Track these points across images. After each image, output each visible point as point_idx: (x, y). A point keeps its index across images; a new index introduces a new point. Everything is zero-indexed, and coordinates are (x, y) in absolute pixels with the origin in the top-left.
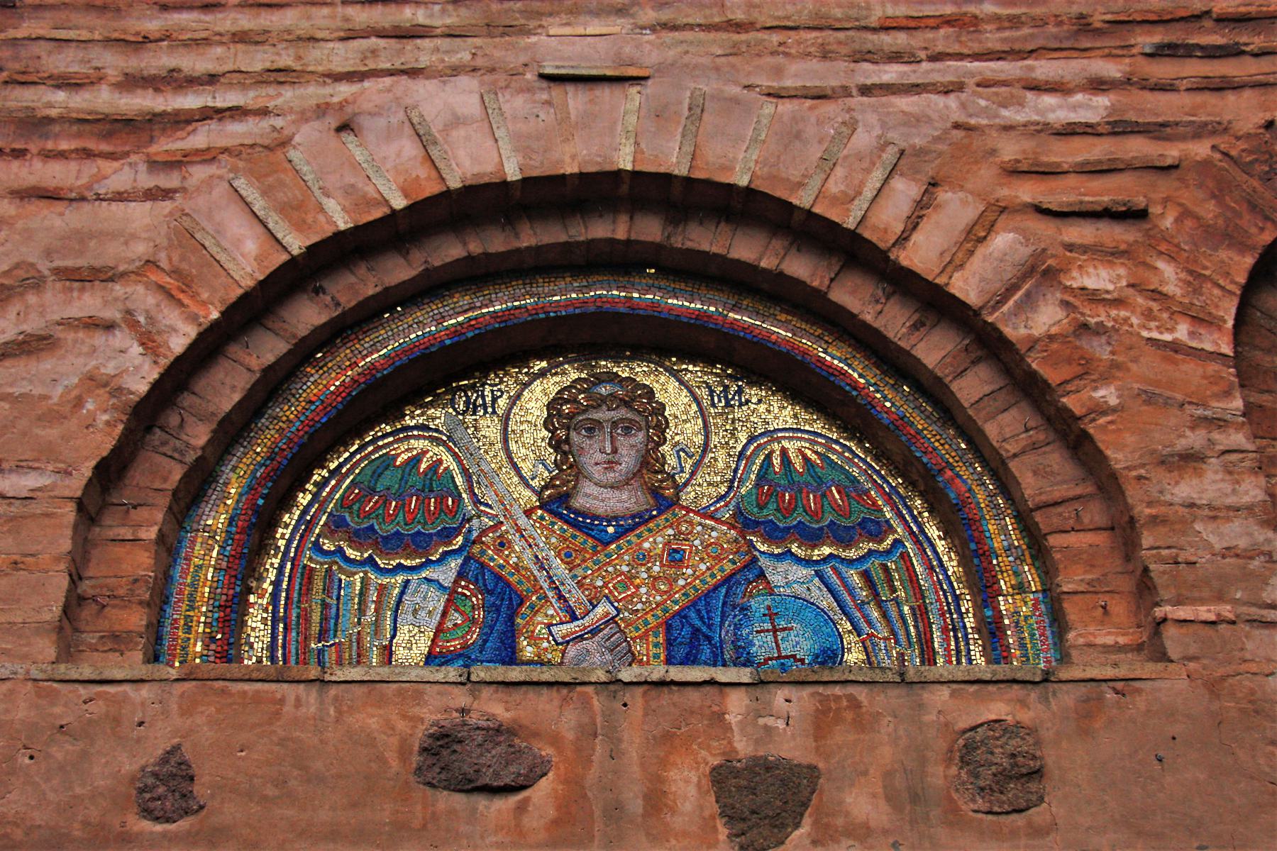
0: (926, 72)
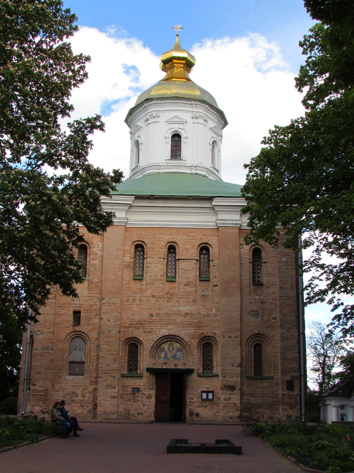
0: (187, 329)
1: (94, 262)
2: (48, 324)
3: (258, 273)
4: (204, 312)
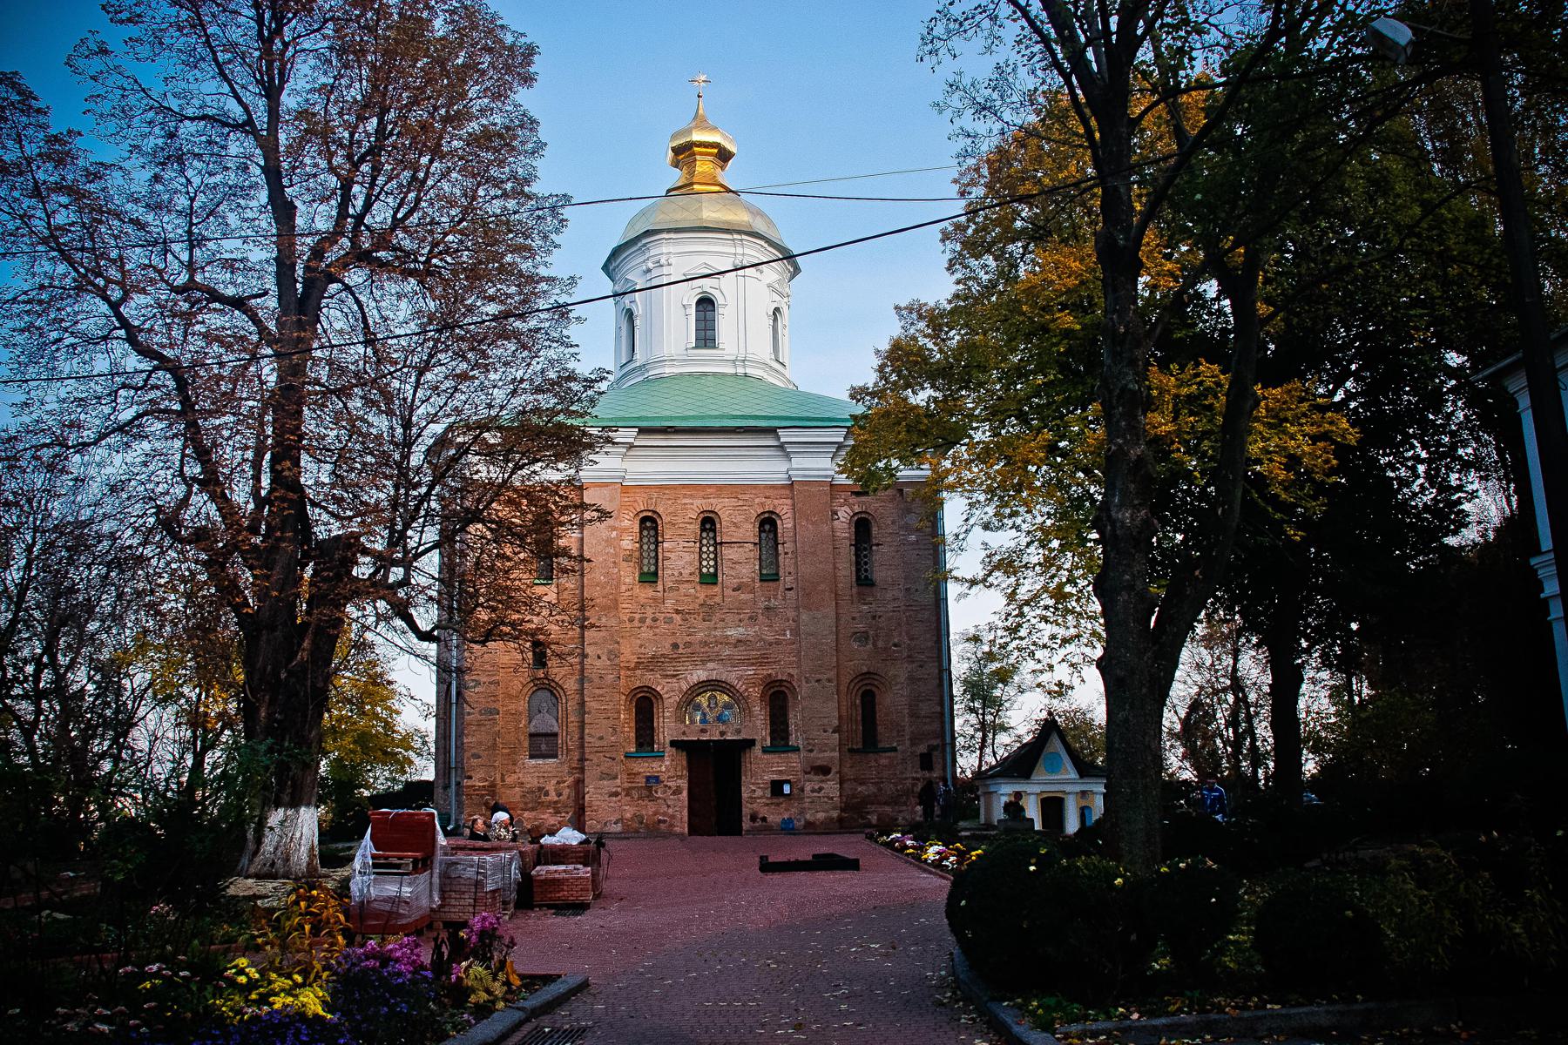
3: (866, 563)
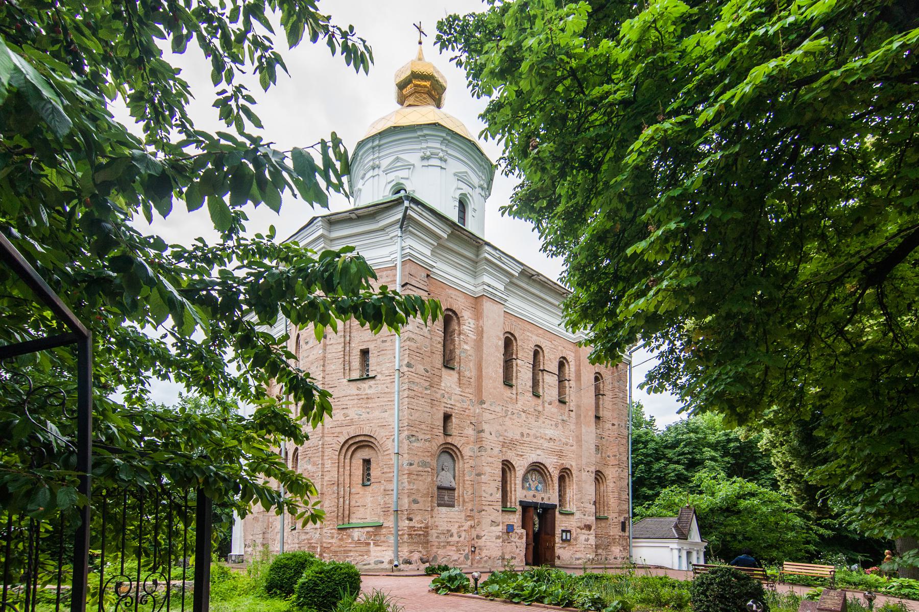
1: (466, 347)
2: (423, 426)
4: (564, 440)
